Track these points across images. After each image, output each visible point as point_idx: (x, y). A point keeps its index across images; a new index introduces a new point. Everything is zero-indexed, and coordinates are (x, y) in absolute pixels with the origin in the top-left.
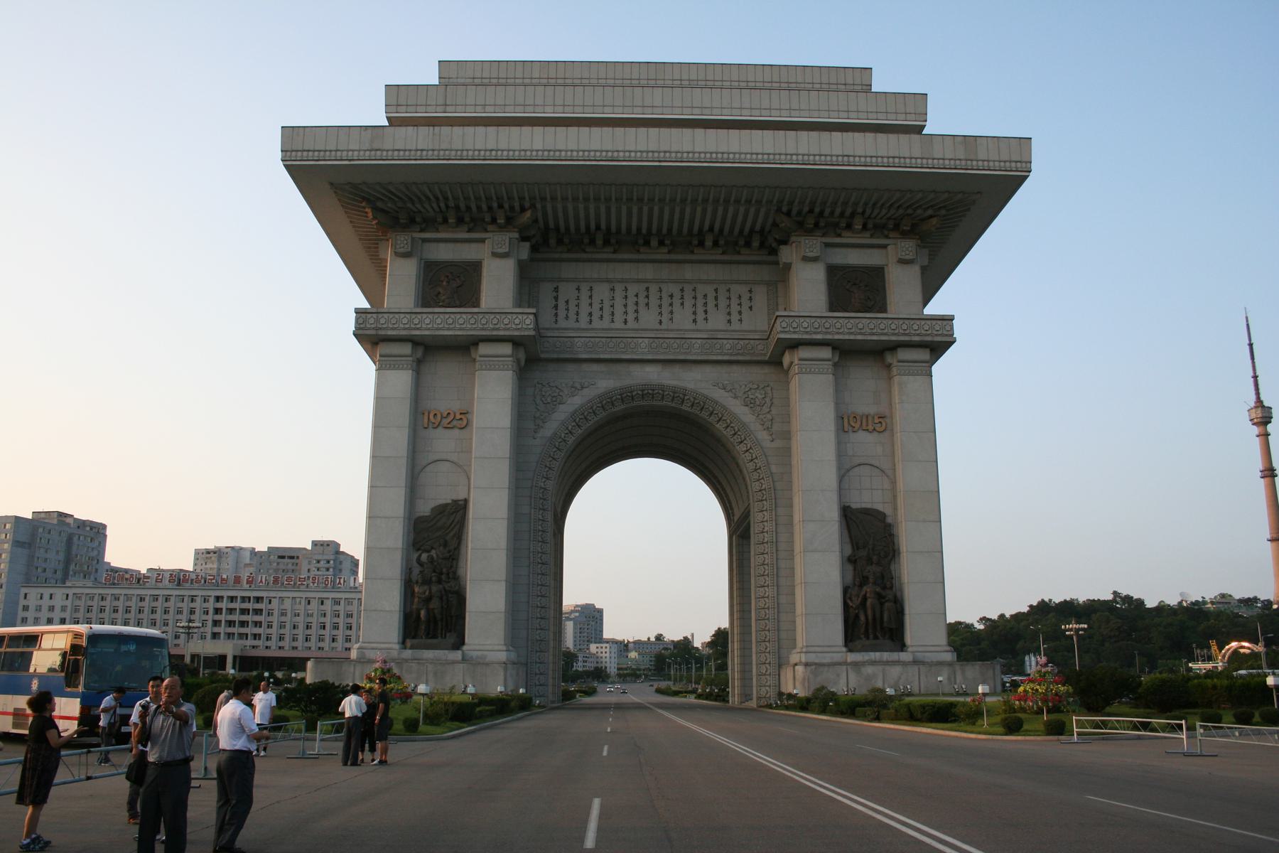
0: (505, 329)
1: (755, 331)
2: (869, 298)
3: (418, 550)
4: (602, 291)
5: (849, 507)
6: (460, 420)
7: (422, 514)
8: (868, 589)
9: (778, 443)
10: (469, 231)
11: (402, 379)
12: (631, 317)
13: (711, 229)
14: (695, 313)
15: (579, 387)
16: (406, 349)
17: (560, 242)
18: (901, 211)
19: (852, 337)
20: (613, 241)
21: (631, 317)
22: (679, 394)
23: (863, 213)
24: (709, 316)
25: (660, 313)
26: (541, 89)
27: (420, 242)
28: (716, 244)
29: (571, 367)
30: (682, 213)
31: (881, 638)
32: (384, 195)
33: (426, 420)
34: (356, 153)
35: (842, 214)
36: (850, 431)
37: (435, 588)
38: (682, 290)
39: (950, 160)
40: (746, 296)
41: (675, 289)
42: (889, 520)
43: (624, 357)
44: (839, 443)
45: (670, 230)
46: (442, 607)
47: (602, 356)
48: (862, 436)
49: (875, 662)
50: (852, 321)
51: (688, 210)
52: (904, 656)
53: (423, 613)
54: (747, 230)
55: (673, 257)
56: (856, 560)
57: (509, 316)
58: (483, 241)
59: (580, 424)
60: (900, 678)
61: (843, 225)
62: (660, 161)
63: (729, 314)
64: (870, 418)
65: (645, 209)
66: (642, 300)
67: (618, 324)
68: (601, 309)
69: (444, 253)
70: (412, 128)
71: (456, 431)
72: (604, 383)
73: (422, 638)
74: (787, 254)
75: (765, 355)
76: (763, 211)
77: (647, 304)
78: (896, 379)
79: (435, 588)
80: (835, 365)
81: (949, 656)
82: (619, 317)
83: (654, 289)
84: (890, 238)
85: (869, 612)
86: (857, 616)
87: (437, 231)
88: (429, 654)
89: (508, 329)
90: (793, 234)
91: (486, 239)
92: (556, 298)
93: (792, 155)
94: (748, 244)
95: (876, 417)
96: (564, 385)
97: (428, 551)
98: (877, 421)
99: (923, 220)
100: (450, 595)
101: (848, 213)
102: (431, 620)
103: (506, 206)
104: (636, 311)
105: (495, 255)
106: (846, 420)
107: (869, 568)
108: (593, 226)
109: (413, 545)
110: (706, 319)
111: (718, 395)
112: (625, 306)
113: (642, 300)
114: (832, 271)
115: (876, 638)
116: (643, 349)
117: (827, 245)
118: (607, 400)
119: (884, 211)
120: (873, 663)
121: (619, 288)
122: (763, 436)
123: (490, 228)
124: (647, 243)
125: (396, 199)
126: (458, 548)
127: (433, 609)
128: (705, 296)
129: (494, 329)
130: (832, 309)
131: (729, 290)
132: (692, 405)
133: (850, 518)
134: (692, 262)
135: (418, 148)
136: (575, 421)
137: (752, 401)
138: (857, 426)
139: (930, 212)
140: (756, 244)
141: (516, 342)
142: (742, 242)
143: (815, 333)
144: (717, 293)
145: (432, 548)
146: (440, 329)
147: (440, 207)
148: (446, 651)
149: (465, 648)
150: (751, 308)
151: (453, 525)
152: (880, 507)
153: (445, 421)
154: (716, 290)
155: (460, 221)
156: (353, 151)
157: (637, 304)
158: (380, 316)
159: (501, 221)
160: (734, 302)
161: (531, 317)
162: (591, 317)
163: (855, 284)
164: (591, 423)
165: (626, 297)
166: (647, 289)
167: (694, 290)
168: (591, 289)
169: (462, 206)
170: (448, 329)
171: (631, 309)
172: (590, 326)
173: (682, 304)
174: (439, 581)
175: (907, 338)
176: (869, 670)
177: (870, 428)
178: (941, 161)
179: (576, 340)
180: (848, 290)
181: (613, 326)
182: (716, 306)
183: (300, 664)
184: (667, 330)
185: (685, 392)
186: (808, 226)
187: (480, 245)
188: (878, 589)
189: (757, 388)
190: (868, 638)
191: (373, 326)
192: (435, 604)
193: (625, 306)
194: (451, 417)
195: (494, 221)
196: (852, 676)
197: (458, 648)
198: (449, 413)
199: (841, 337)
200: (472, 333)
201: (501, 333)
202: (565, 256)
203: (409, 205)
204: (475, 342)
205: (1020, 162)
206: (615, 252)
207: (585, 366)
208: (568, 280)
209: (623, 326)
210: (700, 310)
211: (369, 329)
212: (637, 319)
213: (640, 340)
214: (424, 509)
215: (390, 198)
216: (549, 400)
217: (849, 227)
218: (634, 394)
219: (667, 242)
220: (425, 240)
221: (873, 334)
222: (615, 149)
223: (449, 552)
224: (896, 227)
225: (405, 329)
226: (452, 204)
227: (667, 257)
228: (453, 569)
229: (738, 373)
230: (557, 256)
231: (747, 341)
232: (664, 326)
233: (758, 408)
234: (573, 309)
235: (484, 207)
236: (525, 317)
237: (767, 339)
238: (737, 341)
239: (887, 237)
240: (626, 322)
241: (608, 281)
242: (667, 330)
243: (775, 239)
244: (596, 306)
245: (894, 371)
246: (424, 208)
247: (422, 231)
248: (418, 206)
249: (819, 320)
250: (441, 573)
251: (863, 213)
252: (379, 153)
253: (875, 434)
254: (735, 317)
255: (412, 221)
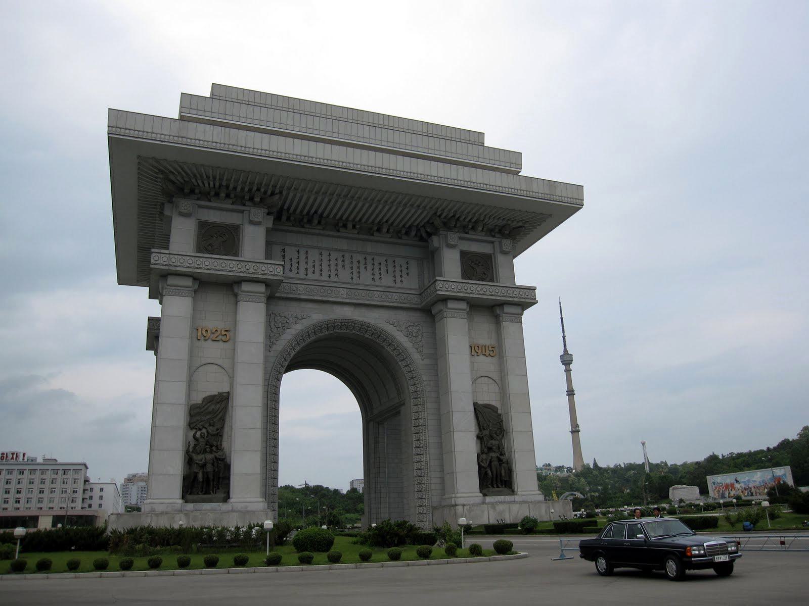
0: (262, 274)
1: (411, 289)
2: (484, 273)
3: (191, 429)
4: (314, 255)
5: (477, 403)
6: (226, 336)
7: (195, 402)
8: (493, 455)
9: (427, 361)
10: (233, 204)
12: (333, 274)
13: (387, 221)
14: (373, 274)
16: (189, 282)
17: (288, 219)
18: (505, 222)
19: (480, 296)
20: (323, 222)
21: (333, 274)
22: (364, 327)
23: (484, 220)
24: (382, 277)
25: (352, 272)
26: (285, 113)
27: (197, 206)
28: (388, 231)
29: (295, 304)
30: (376, 207)
31: (500, 486)
32: (176, 170)
33: (200, 333)
34: (167, 137)
35: (470, 221)
36: (476, 355)
37: (209, 457)
38: (365, 259)
39: (542, 194)
40: (404, 267)
41: (360, 257)
42: (499, 412)
43: (331, 299)
44: (472, 363)
45: (360, 220)
46: (214, 471)
47: (316, 298)
48: (482, 358)
49: (501, 502)
50: (480, 286)
51: (380, 207)
52: (517, 498)
53: (200, 476)
54: (407, 226)
55: (361, 236)
56: (483, 437)
57: (266, 265)
58: (242, 212)
59: (299, 343)
60: (518, 512)
61: (470, 227)
62: (376, 173)
63: (395, 277)
65: (354, 203)
66: (340, 263)
67: (325, 278)
68: (314, 266)
69: (214, 217)
70: (209, 126)
71: (221, 343)
72: (317, 316)
73: (198, 494)
74: (435, 241)
75: (418, 304)
76: (425, 213)
78: (505, 324)
79: (209, 457)
80: (468, 313)
81: (541, 498)
82: (325, 273)
83: (347, 256)
84: (496, 237)
85: (494, 470)
86: (486, 473)
87: (210, 201)
88: (207, 506)
89: (265, 274)
90: (441, 229)
91: (244, 210)
93: (454, 180)
94: (407, 233)
95: (490, 347)
96: (290, 316)
97: (200, 430)
98: (491, 349)
99: (514, 228)
100: (220, 462)
101: (473, 220)
102: (207, 480)
103: (262, 190)
104: (337, 270)
105: (252, 223)
106: (473, 348)
107: (491, 441)
108: (313, 211)
109: (189, 425)
110: (381, 279)
111: (390, 329)
112: (329, 266)
113: (340, 263)
114: (463, 254)
115: (498, 487)
116: (342, 295)
117: (461, 238)
118: (318, 328)
119: (496, 221)
120: (501, 503)
121: (325, 254)
122: (416, 356)
123: (247, 203)
124: (345, 226)
125: (184, 174)
126: (223, 427)
127: (207, 472)
128: (380, 263)
129: (254, 273)
130: (463, 278)
131: (394, 261)
132: (372, 334)
133: (478, 411)
134: (371, 241)
135: (214, 141)
136: (297, 341)
137: (411, 333)
138: (479, 352)
139: (520, 224)
140: (413, 233)
141: (267, 283)
142: (403, 232)
143: (459, 292)
144: (387, 262)
145: (204, 427)
146: (216, 270)
147: (214, 185)
148: (221, 503)
149: (232, 500)
150: (408, 274)
151: (219, 412)
152: (493, 403)
153: (213, 337)
154: (386, 261)
155: (228, 196)
156: (165, 135)
157: (337, 265)
158: (171, 256)
159: (257, 199)
160: (398, 270)
161: (281, 267)
162: (307, 271)
163: (476, 264)
164: (306, 343)
165: (330, 260)
166: (343, 256)
167: (373, 259)
168: (307, 253)
169: (231, 186)
170: (222, 271)
171: (333, 268)
172: (307, 278)
173: (366, 268)
174: (211, 452)
175: (511, 299)
176: (500, 507)
178: (537, 194)
179: (299, 286)
180: (472, 267)
181: (321, 278)
182: (387, 270)
183: (34, 520)
184: (356, 284)
185: (368, 325)
186: (451, 225)
187: (240, 215)
188: (499, 456)
189: (413, 326)
190: (493, 487)
191: (165, 263)
192: (209, 468)
193: (329, 266)
194: (219, 333)
195: (251, 199)
196: (491, 512)
198: (217, 330)
199: (475, 296)
200: (238, 274)
201: (260, 276)
202: (291, 228)
203: (194, 180)
204: (239, 281)
205: (578, 199)
206: (323, 229)
207: (303, 304)
208: (291, 245)
209: (327, 279)
210: (377, 272)
211: (163, 265)
212: (337, 275)
213: (342, 289)
214: (198, 399)
215: (179, 172)
216: (280, 325)
217: (473, 228)
218: (336, 324)
219: (358, 226)
220: (200, 207)
221: (492, 295)
222: (347, 161)
223: (217, 430)
224: (500, 232)
225: (189, 267)
226: (224, 183)
227: (357, 236)
228: (219, 444)
229: (402, 316)
230: (286, 228)
231: (407, 295)
232: (354, 281)
233: (415, 339)
234: (295, 265)
235: (246, 189)
236: (277, 267)
237: (420, 295)
238: (401, 295)
239: (494, 236)
240: (330, 277)
241: (319, 248)
242: (356, 284)
243: (427, 232)
244: (310, 264)
245: (501, 318)
246: (203, 184)
247: (198, 199)
248: (200, 182)
249: (461, 284)
250: (212, 446)
251: (484, 220)
252: (185, 140)
253: (490, 358)
254: (398, 279)
255: (192, 191)
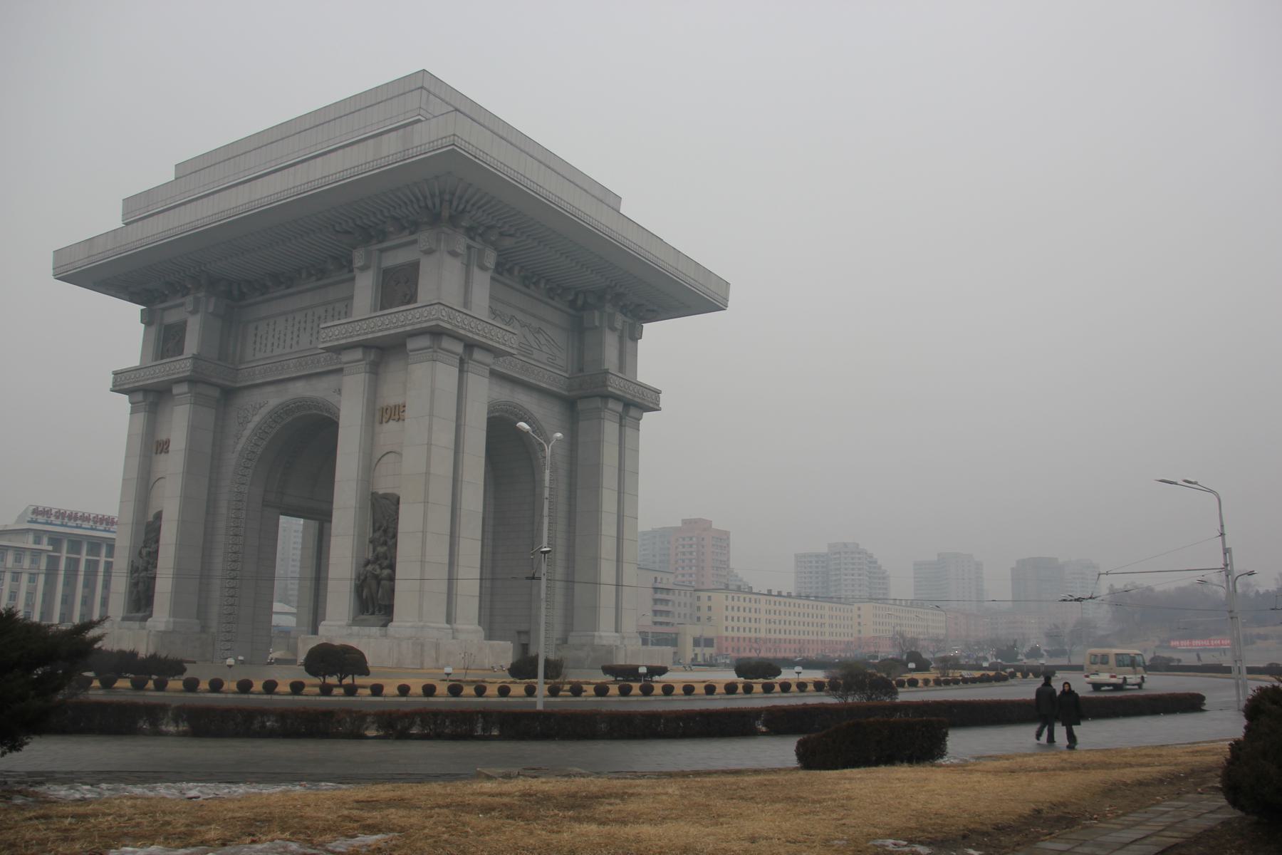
8: (369, 568)
11: (141, 417)
15: (258, 406)
64: (397, 408)
68: (279, 339)
72: (272, 399)
77: (305, 329)
92: (256, 335)
104: (298, 336)
115: (373, 613)
138: (388, 416)
157: (299, 330)
177: (397, 417)
197: (145, 619)
206: (288, 287)
212: (298, 343)
218: (291, 406)
